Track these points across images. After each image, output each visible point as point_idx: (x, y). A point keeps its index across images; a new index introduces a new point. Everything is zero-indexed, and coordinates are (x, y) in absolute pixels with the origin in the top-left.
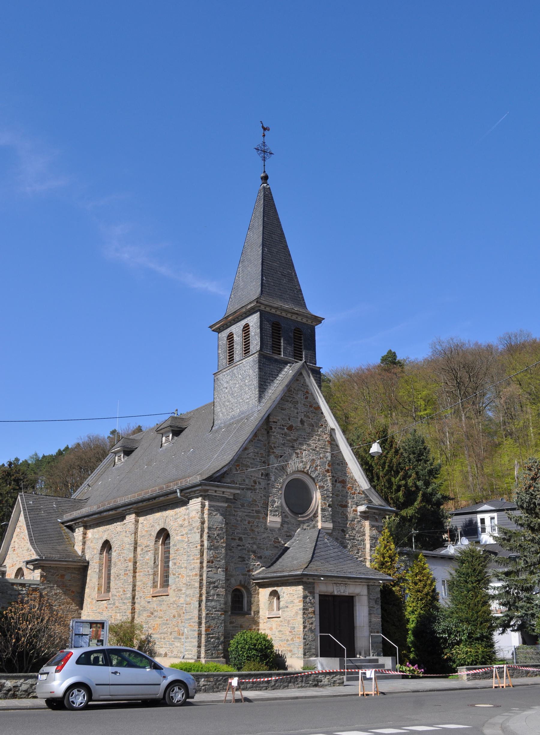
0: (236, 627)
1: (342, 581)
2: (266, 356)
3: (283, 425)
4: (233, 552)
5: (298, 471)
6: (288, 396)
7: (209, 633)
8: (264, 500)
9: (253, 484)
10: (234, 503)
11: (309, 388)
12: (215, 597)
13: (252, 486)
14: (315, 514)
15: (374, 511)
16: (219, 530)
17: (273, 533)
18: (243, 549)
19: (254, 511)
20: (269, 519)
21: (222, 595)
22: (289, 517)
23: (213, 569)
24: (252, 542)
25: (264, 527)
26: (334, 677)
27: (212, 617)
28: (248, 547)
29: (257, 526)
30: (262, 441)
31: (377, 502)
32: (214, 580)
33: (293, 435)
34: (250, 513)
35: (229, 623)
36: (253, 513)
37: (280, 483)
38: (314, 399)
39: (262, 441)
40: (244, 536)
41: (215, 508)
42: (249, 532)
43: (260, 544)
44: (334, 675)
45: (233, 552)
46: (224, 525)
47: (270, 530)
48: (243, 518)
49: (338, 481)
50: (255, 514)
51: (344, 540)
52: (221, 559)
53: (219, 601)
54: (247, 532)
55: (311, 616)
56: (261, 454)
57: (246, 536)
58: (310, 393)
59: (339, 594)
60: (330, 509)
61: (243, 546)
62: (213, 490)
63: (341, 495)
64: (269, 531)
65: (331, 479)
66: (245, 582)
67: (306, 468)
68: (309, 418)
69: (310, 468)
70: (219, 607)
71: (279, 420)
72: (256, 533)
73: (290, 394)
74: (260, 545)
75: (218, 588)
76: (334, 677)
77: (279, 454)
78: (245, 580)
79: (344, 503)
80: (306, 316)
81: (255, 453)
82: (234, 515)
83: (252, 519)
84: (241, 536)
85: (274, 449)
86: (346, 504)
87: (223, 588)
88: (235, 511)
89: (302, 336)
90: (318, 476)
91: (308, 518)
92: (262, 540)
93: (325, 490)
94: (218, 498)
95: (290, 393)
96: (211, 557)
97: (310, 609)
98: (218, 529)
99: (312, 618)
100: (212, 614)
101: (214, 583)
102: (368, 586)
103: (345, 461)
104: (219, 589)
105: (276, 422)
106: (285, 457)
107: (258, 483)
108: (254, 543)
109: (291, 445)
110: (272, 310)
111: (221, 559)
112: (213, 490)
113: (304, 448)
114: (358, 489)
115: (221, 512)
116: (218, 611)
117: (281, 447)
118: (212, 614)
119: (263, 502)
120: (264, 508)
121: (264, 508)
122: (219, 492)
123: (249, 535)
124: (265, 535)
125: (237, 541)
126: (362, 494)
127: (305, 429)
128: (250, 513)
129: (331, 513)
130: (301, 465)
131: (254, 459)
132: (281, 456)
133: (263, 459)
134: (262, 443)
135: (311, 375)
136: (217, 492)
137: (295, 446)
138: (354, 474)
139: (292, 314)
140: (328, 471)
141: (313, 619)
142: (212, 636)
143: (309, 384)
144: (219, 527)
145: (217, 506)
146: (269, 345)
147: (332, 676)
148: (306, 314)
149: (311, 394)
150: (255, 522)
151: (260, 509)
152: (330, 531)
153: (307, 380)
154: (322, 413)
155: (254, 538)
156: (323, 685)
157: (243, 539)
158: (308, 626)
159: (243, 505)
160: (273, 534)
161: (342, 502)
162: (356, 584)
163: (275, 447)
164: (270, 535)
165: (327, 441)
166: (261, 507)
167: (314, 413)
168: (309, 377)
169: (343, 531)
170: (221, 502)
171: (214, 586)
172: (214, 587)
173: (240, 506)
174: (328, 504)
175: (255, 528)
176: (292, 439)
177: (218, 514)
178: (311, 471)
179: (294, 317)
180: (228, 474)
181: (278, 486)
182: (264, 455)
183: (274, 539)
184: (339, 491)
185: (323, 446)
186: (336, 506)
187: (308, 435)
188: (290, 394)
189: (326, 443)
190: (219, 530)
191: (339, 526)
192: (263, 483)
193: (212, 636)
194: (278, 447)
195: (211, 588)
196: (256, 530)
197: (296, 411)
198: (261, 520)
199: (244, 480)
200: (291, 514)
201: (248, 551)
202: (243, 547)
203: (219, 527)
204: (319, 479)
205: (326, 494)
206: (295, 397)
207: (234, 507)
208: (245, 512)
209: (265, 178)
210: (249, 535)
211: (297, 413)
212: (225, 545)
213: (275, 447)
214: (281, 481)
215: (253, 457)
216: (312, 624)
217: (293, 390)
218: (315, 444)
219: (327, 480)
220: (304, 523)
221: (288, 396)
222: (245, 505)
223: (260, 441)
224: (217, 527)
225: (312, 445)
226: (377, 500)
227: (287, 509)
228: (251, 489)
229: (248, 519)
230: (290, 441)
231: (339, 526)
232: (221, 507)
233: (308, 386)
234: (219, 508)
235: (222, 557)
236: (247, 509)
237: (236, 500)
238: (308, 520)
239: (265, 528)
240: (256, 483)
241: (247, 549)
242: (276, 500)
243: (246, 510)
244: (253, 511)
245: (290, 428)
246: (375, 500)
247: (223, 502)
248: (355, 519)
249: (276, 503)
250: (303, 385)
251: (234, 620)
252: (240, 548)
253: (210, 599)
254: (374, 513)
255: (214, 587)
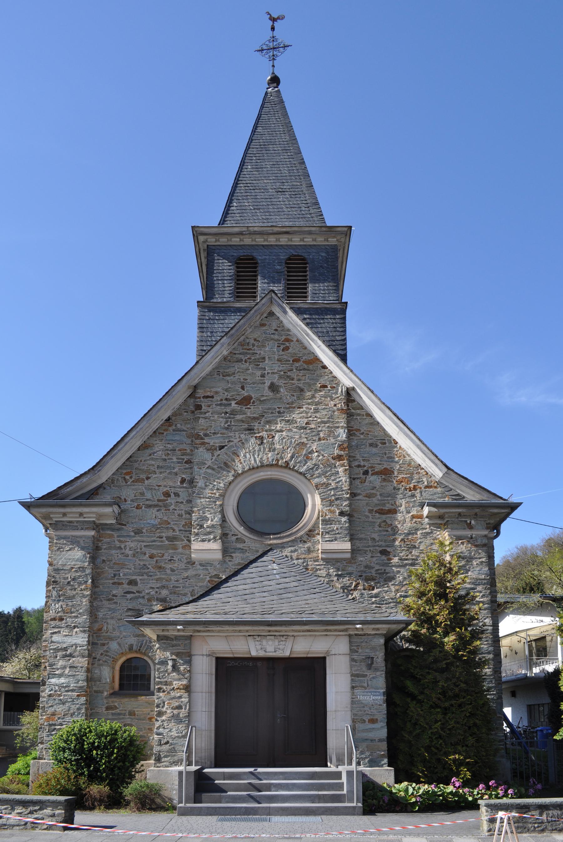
0: (119, 714)
1: (270, 631)
2: (216, 307)
3: (226, 399)
4: (116, 603)
5: (262, 466)
6: (240, 354)
7: (54, 723)
8: (185, 519)
9: (163, 498)
10: (118, 530)
11: (290, 333)
12: (67, 671)
13: (159, 500)
14: (310, 531)
15: (460, 510)
16: (76, 571)
17: (209, 568)
18: (139, 597)
19: (164, 539)
20: (196, 545)
21: (82, 667)
22: (246, 541)
23: (62, 630)
24: (158, 585)
25: (185, 561)
26: (36, 811)
27: (60, 700)
28: (148, 594)
29: (170, 560)
30: (184, 431)
31: (473, 496)
32: (65, 646)
33: (251, 411)
34: (154, 541)
35: (104, 709)
36: (162, 542)
37: (218, 489)
38: (306, 348)
39: (184, 431)
40: (141, 577)
41: (70, 540)
42: (152, 570)
43: (178, 587)
44: (37, 808)
45: (116, 603)
46: (86, 564)
47: (201, 565)
48: (139, 550)
49: (370, 473)
50: (167, 542)
51: (388, 569)
52: (80, 614)
53: (74, 676)
54: (146, 571)
55: (178, 695)
56: (180, 450)
57: (145, 577)
58: (295, 339)
59: (262, 654)
60: (344, 519)
61: (138, 592)
62: (59, 513)
63: (381, 495)
64: (199, 567)
65: (346, 470)
66: (141, 647)
67: (282, 459)
68: (293, 379)
69: (292, 457)
70: (75, 685)
71: (217, 393)
72: (169, 571)
73: (246, 349)
74: (178, 589)
75: (73, 657)
76: (36, 811)
77: (217, 445)
78: (142, 644)
79: (388, 507)
80: (308, 231)
81: (167, 450)
82: (120, 548)
83: (159, 551)
84: (134, 577)
85: (205, 438)
86: (393, 507)
87: (83, 657)
88: (120, 541)
89: (308, 265)
90: (312, 469)
91: (293, 538)
92: (181, 581)
93: (331, 490)
94: (75, 524)
95: (245, 347)
96: (58, 612)
97: (174, 683)
98: (74, 570)
99: (180, 697)
100: (60, 695)
101: (65, 649)
102: (350, 636)
103: (391, 437)
104: (74, 659)
105: (212, 397)
106: (232, 446)
107: (172, 495)
108: (163, 587)
109: (246, 426)
110: (234, 239)
111: (80, 614)
112: (59, 513)
113: (278, 428)
114: (425, 479)
115: (83, 545)
116: (73, 691)
117: (221, 433)
118: (60, 695)
119: (183, 523)
120: (186, 531)
121: (186, 531)
122: (71, 515)
123: (151, 576)
124: (190, 573)
125: (125, 586)
126: (436, 487)
127: (281, 399)
128: (154, 541)
129: (347, 525)
130: (270, 455)
131: (165, 460)
132: (221, 448)
133: (186, 458)
134: (185, 433)
135: (288, 309)
136: (85, 516)
137: (255, 428)
138: (414, 457)
139: (276, 236)
140: (339, 457)
141: (183, 700)
142: (59, 727)
143: (290, 327)
144: (76, 567)
145: (72, 536)
146: (226, 292)
147: (31, 808)
148: (307, 229)
149: (298, 341)
150: (166, 554)
151: (178, 533)
152: (348, 556)
153: (285, 321)
154: (325, 367)
155: (163, 579)
156: (5, 825)
157: (139, 582)
158: (168, 711)
159: (138, 532)
160: (207, 570)
161: (384, 505)
162: (315, 636)
163: (206, 435)
164: (200, 572)
165: (338, 410)
166: (180, 530)
167: (304, 369)
168: (285, 312)
169: (384, 552)
170: (82, 529)
171: (63, 655)
172: (66, 656)
173: (132, 534)
174: (337, 511)
175: (165, 563)
176: (249, 417)
177: (76, 549)
178: (295, 463)
179: (284, 240)
180: (105, 488)
181: (215, 494)
182: (188, 451)
183: (211, 577)
184: (374, 488)
185: (326, 420)
186: (367, 513)
187: (288, 406)
188: (246, 349)
189: (336, 413)
190: (76, 571)
191: (374, 546)
192: (184, 496)
193: (59, 727)
194: (214, 433)
195: (58, 658)
196: (169, 566)
197: (259, 373)
198: (180, 550)
199: (142, 494)
200: (255, 538)
201: (149, 600)
202: (137, 594)
203: (76, 567)
204: (317, 472)
205: (333, 495)
206: (258, 352)
207: (118, 536)
208: (143, 542)
209: (275, 80)
210: (151, 576)
211: (263, 376)
212: (89, 593)
213: (206, 435)
214: (222, 485)
215: (164, 457)
216: (179, 707)
217: (252, 341)
218: (307, 418)
219: (337, 473)
220: (284, 547)
221: (240, 354)
222: (144, 531)
223: (180, 431)
224: (72, 568)
225: (299, 420)
226: (471, 492)
227: (241, 529)
228: (155, 506)
229: (148, 551)
230: (243, 421)
231: (374, 546)
232: (81, 537)
233: (289, 330)
234: (78, 539)
235: (81, 611)
236: (149, 537)
237: (125, 525)
238: (292, 541)
239: (188, 563)
240: (169, 496)
241: (146, 597)
242: (208, 516)
243: (145, 539)
244: (162, 538)
245: (246, 401)
246: (468, 494)
247: (87, 529)
248: (417, 529)
249: (209, 522)
250: (276, 330)
251: (116, 704)
252: (129, 596)
253: (55, 674)
254: (460, 514)
255: (66, 656)
